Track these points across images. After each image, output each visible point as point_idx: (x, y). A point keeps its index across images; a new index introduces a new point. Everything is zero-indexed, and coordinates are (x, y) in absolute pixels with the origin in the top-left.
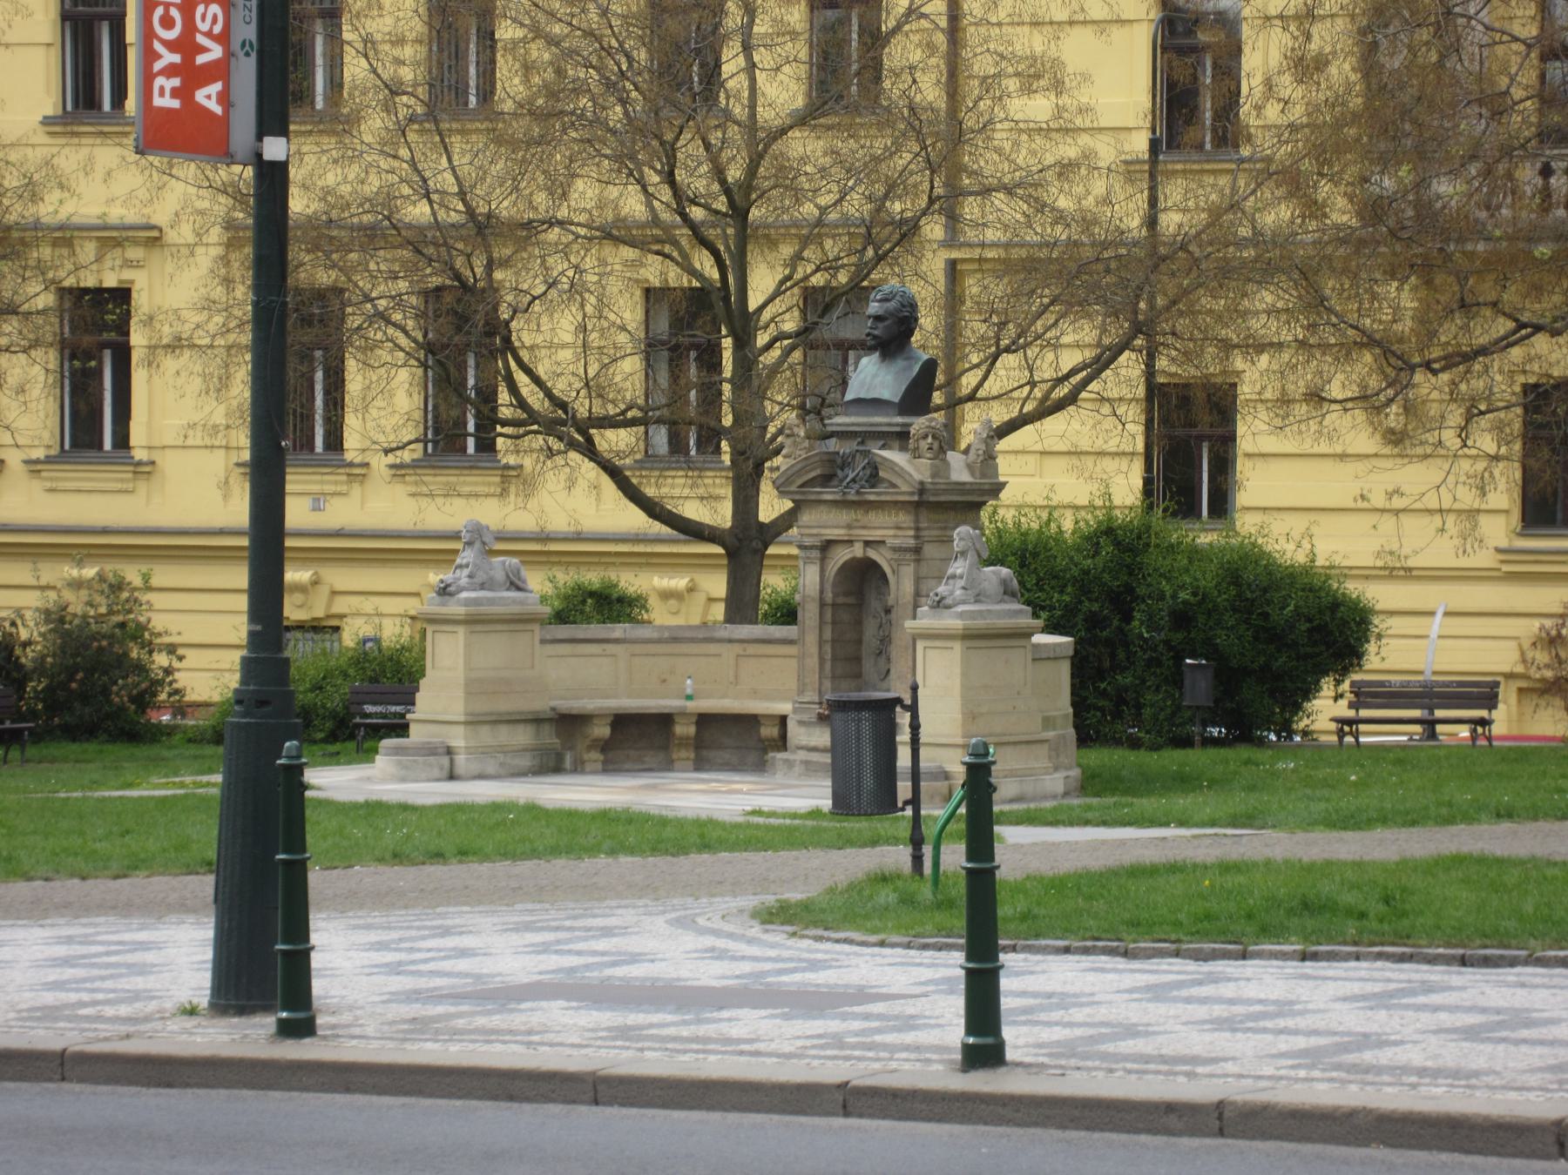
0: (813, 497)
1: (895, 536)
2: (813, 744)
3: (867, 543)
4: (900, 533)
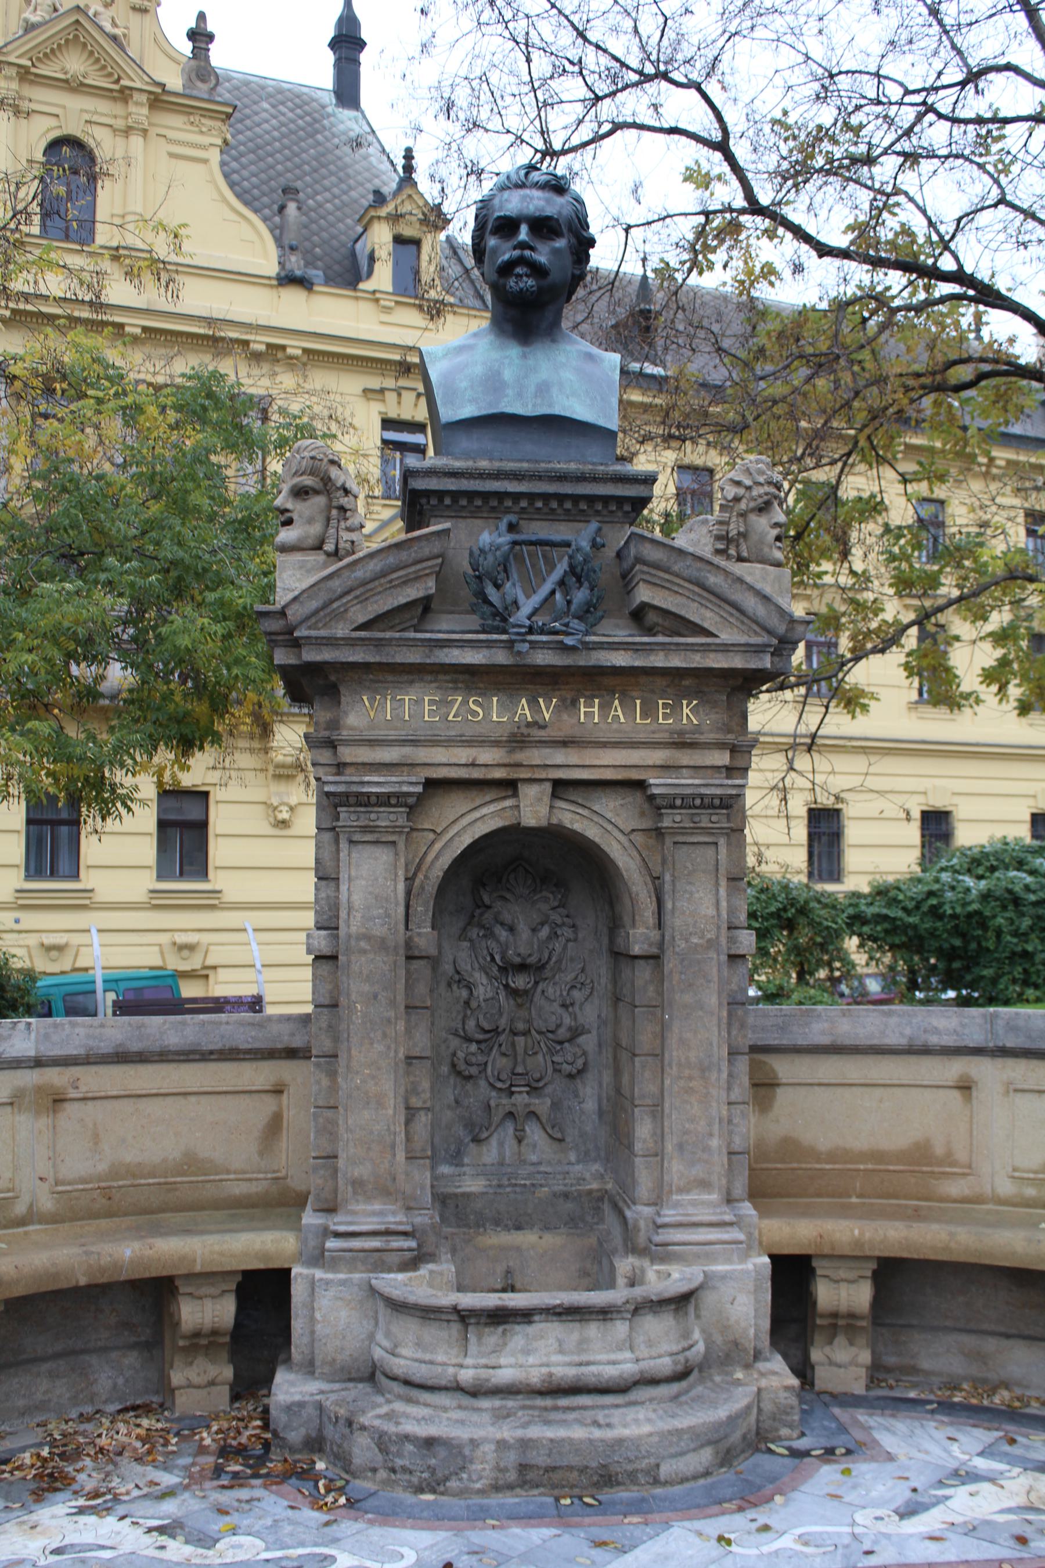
0: (413, 657)
2: (505, 1375)
3: (561, 788)
4: (686, 758)
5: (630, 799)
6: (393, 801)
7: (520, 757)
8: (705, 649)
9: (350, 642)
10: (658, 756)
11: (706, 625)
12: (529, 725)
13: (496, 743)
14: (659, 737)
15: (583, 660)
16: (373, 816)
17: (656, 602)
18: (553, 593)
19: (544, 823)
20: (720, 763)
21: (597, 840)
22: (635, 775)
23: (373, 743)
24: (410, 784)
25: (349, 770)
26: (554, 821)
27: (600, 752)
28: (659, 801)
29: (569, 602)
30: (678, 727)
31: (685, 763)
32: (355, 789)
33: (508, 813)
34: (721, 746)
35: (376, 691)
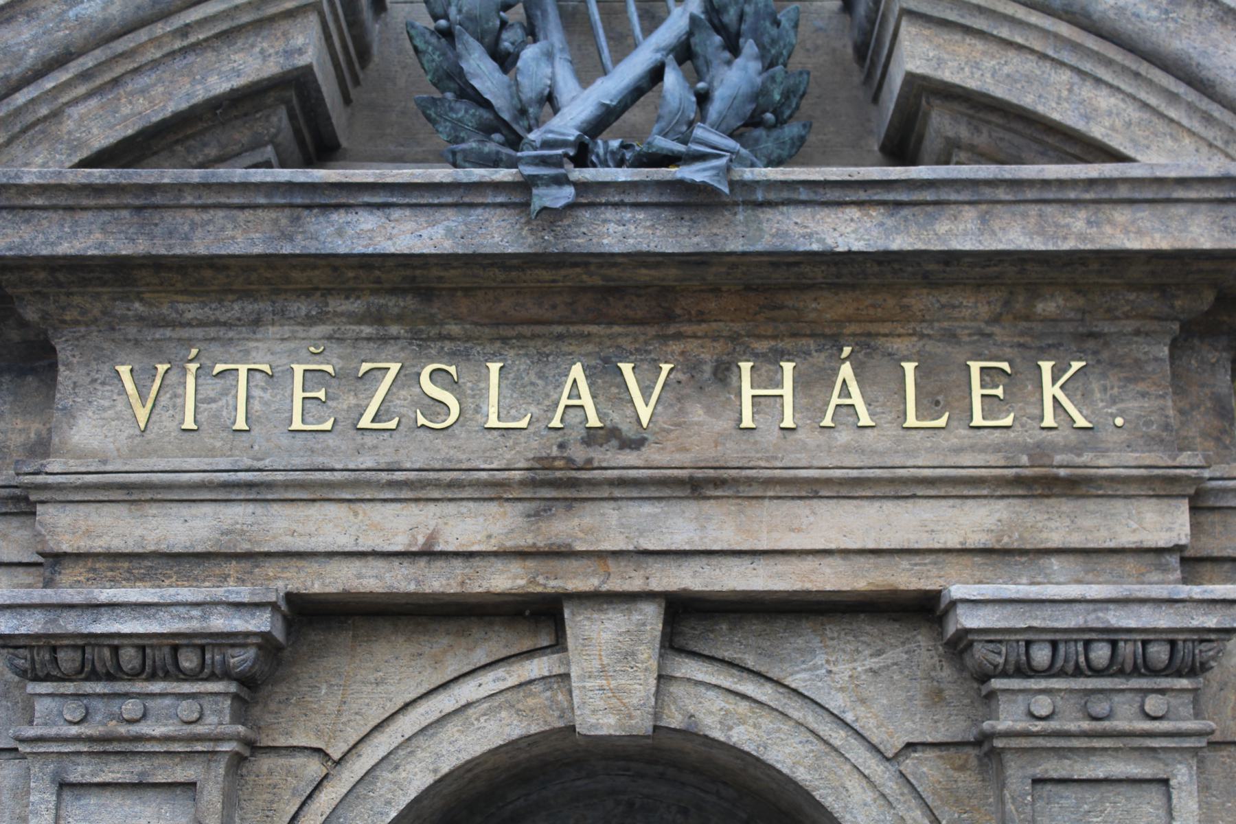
0: (242, 237)
1: (996, 555)
3: (690, 619)
4: (1057, 524)
5: (896, 654)
6: (188, 661)
7: (568, 528)
8: (1103, 196)
9: (61, 199)
10: (975, 521)
11: (1097, 131)
12: (592, 437)
13: (494, 490)
14: (972, 462)
15: (737, 235)
16: (131, 708)
17: (949, 75)
18: (656, 74)
19: (642, 724)
20: (1162, 539)
21: (802, 775)
22: (907, 578)
23: (137, 493)
24: (234, 609)
25: (68, 575)
26: (674, 720)
27: (801, 509)
28: (981, 652)
29: (703, 99)
30: (1032, 437)
31: (1055, 539)
32: (71, 624)
33: (539, 698)
34: (1161, 486)
35: (157, 351)
